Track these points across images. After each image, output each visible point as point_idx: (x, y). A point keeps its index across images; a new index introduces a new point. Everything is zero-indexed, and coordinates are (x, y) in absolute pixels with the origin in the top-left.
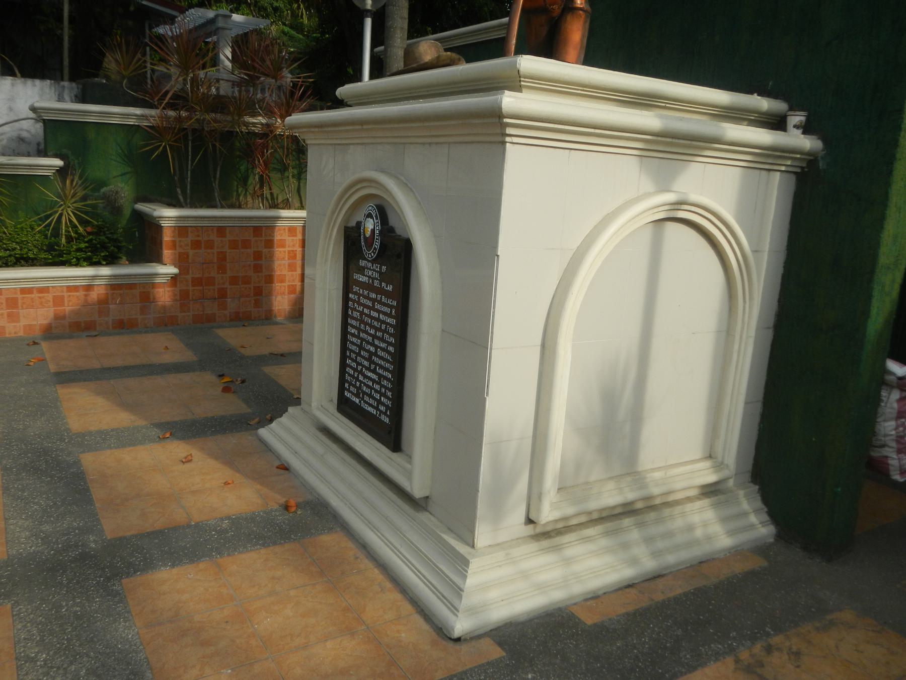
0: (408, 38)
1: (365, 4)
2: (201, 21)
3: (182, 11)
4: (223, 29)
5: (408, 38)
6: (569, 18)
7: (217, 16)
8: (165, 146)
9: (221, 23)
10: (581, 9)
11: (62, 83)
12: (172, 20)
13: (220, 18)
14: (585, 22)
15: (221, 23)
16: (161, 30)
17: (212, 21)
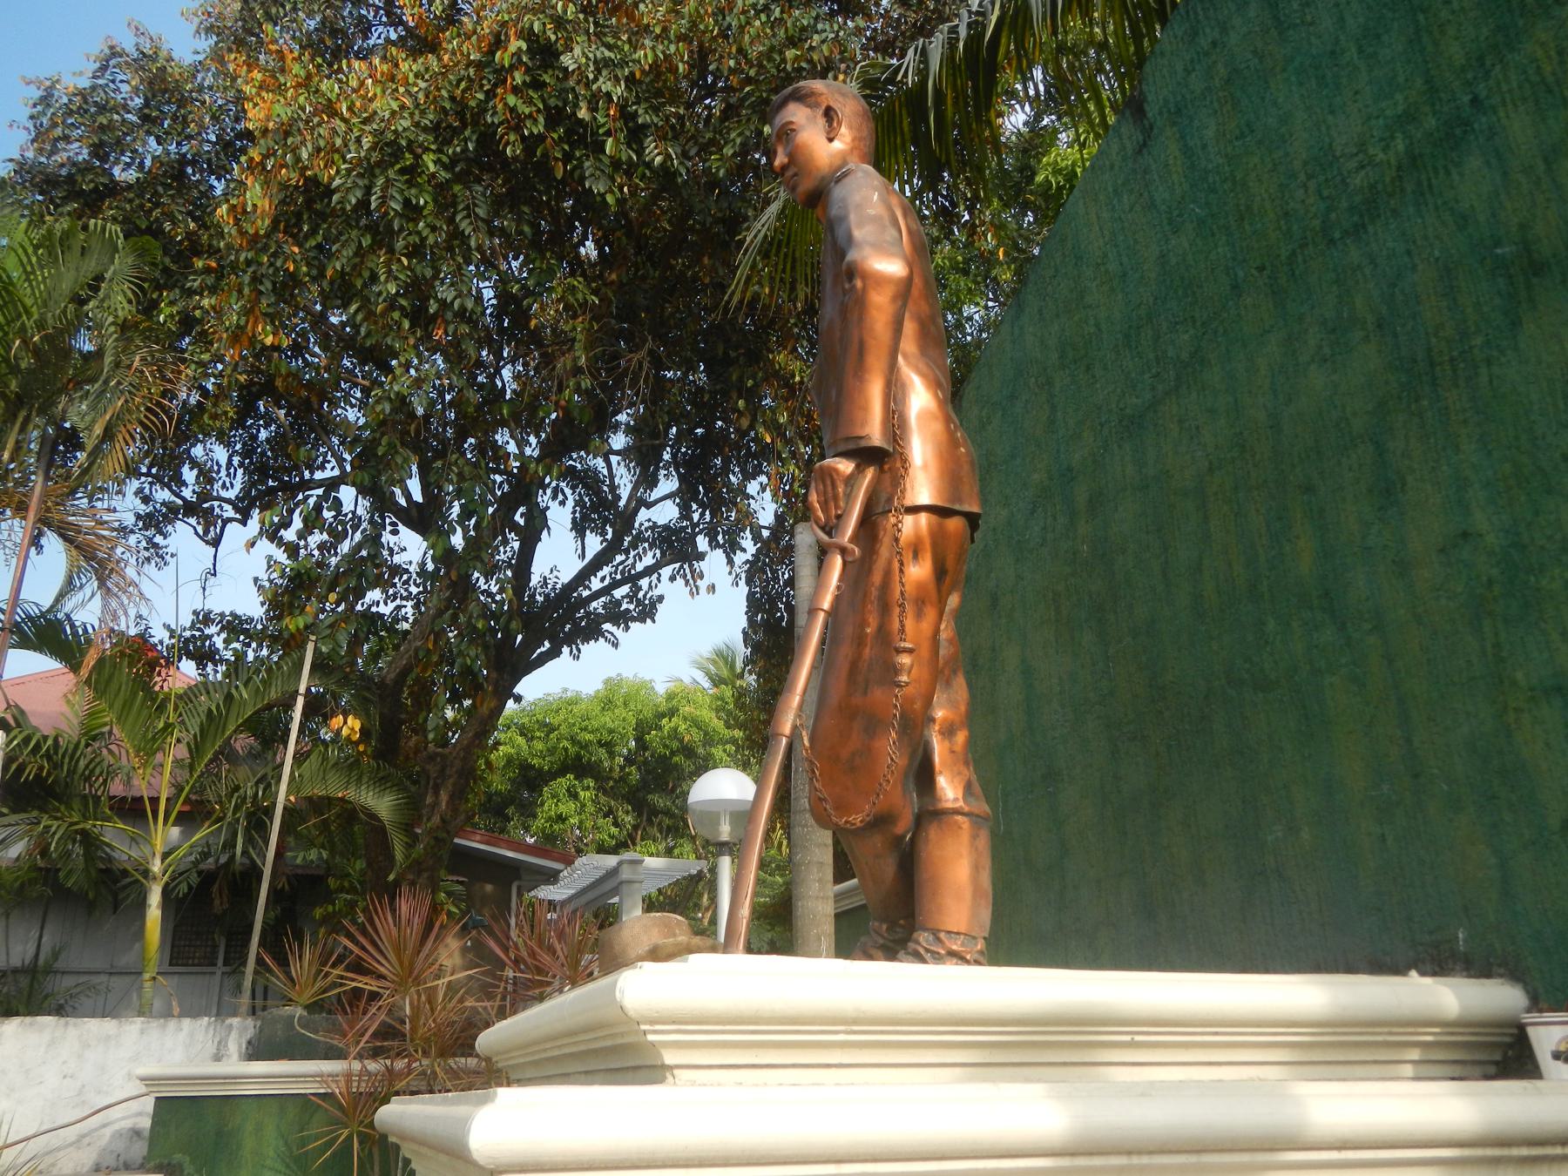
0: (837, 880)
1: (718, 833)
2: (601, 873)
3: (569, 861)
4: (630, 882)
5: (837, 880)
6: (933, 832)
7: (620, 863)
8: (350, 1138)
9: (626, 874)
10: (957, 812)
11: (230, 1021)
12: (552, 877)
13: (625, 866)
14: (974, 837)
15: (626, 874)
16: (546, 892)
17: (613, 872)
